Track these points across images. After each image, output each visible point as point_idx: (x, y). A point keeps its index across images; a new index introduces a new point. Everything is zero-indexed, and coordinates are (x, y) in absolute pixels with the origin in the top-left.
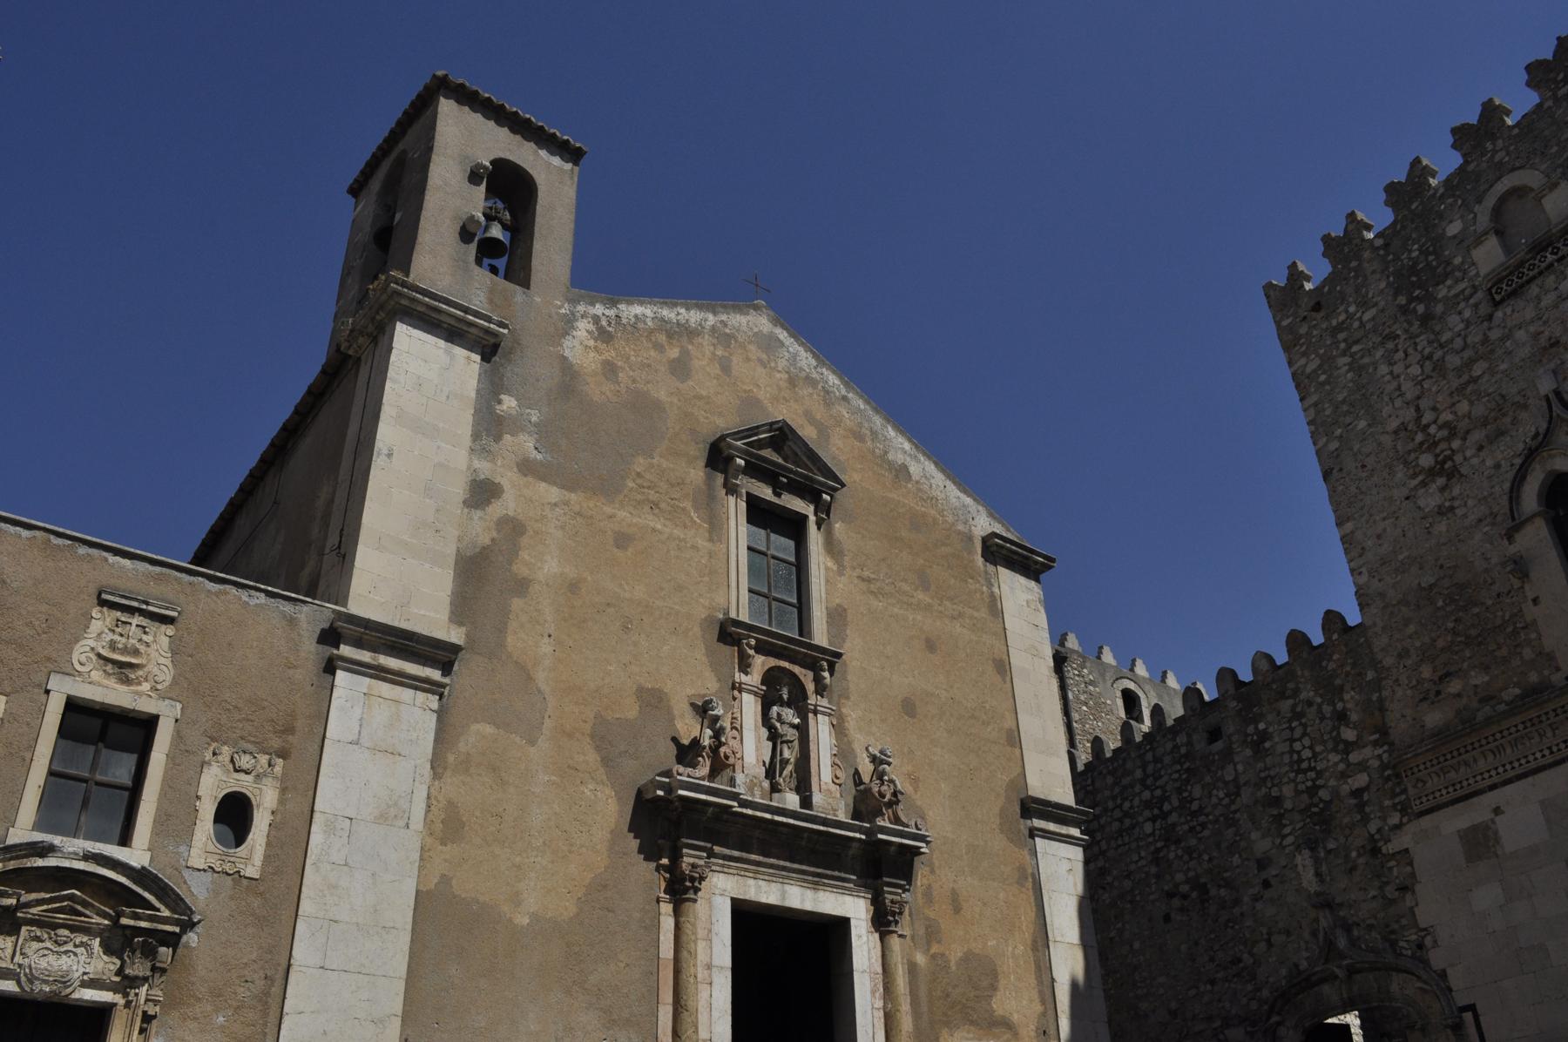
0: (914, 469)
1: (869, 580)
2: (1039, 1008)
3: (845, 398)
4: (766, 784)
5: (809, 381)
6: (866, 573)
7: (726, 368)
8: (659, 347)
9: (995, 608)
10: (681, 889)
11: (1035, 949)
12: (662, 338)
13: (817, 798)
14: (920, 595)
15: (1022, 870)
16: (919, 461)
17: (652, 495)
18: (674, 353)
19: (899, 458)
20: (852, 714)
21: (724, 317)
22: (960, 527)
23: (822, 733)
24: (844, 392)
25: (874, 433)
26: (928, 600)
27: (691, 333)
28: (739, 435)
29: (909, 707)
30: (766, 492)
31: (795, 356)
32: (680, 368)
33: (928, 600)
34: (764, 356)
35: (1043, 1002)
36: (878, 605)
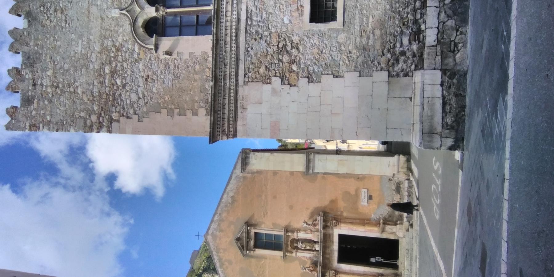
0: (231, 194)
1: (264, 214)
2: (352, 179)
3: (220, 214)
4: (315, 253)
5: (219, 225)
6: (262, 214)
7: (225, 250)
8: (227, 268)
9: (259, 172)
10: (337, 272)
11: (339, 177)
12: (224, 267)
13: (316, 240)
14: (263, 197)
15: (323, 178)
16: (228, 193)
17: (261, 272)
18: (226, 263)
19: (230, 200)
20: (295, 225)
21: (212, 249)
22: (242, 180)
23: (302, 235)
24: (218, 215)
25: (226, 206)
26: (264, 196)
27: (220, 260)
28: (243, 253)
29: (291, 207)
30: (252, 243)
31: (215, 229)
32: (230, 262)
33: (264, 196)
34: (218, 238)
35: (351, 177)
36: (269, 214)
